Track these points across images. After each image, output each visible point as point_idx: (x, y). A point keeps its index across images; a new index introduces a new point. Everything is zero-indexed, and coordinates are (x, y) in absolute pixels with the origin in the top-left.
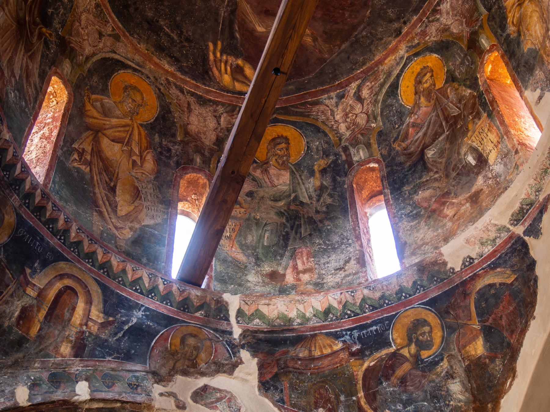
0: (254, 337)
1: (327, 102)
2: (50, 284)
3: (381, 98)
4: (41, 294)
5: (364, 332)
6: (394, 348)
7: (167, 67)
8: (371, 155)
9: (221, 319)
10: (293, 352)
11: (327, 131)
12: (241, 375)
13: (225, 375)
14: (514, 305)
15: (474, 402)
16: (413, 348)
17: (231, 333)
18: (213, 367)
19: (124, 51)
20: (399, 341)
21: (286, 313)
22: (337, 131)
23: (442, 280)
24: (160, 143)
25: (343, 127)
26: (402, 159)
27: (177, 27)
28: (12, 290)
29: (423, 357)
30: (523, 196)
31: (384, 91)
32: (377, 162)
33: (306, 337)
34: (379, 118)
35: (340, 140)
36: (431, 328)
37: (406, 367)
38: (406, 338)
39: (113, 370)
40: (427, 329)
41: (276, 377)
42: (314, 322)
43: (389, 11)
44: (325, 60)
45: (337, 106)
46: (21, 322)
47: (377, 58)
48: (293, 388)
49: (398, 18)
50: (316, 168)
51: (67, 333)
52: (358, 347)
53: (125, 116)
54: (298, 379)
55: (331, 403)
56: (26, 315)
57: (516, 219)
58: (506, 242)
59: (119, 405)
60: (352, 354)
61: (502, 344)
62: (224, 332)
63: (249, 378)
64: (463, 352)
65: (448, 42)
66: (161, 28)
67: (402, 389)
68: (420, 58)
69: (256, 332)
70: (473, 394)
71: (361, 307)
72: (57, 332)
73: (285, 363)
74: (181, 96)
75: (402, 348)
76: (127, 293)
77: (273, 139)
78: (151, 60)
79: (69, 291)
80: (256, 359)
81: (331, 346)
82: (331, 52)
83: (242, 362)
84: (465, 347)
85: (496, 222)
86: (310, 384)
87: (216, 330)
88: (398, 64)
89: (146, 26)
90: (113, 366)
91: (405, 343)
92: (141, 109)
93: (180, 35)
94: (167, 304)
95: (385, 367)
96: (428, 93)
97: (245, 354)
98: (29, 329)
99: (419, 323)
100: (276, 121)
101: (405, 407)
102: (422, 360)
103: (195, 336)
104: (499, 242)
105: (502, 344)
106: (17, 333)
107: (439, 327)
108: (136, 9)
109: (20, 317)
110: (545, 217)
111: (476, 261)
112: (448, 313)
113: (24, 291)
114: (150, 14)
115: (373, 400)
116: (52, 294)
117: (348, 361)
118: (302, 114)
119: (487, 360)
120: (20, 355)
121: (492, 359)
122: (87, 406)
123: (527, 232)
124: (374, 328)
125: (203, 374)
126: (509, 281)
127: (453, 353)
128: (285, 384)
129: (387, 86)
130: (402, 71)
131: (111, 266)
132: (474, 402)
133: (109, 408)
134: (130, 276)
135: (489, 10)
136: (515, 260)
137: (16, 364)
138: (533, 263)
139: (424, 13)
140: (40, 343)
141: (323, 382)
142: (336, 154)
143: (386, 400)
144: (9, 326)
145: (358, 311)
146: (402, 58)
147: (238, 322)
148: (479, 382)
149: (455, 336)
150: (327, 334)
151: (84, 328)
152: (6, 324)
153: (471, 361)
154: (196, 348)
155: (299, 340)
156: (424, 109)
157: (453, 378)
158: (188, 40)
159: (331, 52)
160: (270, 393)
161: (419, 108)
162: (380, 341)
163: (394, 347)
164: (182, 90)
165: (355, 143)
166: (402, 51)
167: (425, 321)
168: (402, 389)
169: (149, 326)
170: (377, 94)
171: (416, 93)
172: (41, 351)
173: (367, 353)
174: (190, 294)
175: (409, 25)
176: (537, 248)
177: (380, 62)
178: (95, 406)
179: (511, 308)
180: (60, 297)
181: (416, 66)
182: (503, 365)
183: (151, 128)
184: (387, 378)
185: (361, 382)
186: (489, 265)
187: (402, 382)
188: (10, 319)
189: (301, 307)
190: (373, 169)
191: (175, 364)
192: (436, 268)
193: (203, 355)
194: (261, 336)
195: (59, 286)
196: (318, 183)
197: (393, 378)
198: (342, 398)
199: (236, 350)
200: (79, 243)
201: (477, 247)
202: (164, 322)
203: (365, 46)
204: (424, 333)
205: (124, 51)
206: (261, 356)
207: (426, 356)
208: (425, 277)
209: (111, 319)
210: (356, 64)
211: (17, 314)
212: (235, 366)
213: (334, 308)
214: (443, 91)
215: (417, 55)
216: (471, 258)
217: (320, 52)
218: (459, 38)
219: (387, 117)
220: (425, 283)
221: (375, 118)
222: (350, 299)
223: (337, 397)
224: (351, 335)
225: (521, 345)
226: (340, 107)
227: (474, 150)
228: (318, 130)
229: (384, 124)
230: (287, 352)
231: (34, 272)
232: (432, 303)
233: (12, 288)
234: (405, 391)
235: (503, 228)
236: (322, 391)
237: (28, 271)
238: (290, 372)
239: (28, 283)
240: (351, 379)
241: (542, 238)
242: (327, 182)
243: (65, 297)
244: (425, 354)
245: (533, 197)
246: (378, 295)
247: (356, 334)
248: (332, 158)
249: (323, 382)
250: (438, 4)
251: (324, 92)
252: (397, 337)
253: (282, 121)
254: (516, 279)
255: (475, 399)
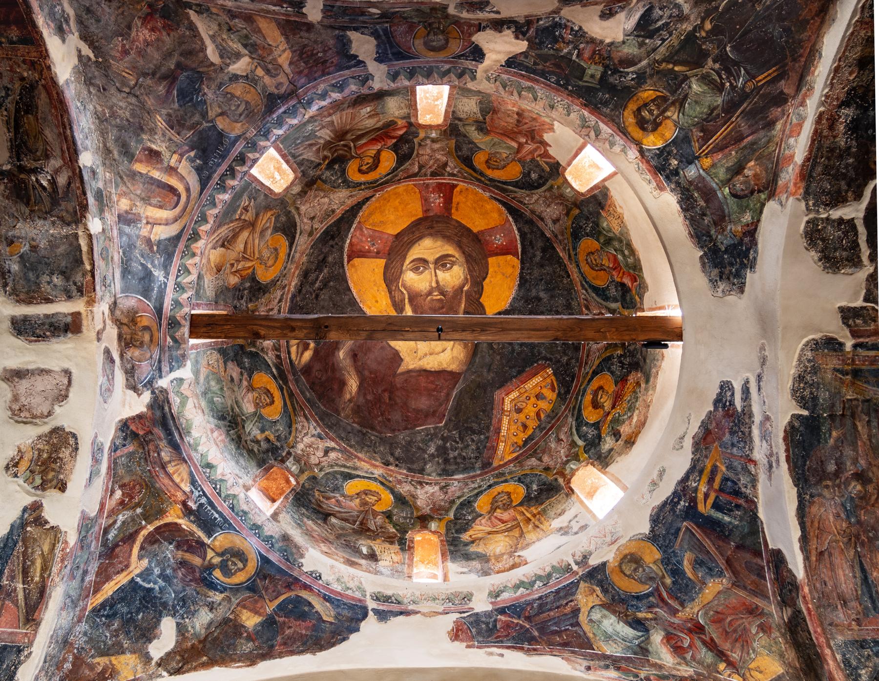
0: (164, 401)
1: (312, 427)
2: (182, 178)
3: (336, 469)
4: (172, 170)
5: (209, 508)
6: (208, 541)
7: (293, 284)
8: (298, 476)
9: (170, 363)
10: (163, 444)
11: (293, 434)
12: (128, 398)
13: (125, 381)
14: (308, 633)
15: (200, 642)
16: (217, 560)
17: (161, 377)
18: (129, 366)
19: (303, 242)
20: (217, 543)
21: (194, 427)
22: (296, 442)
23: (287, 560)
24: (245, 289)
25: (300, 446)
26: (313, 501)
27: (325, 285)
28: (175, 139)
29: (214, 573)
30: (400, 593)
31: (342, 469)
32: (298, 483)
33: (180, 453)
34: (323, 473)
35: (293, 447)
36: (243, 569)
37: (197, 561)
38: (223, 550)
39: (112, 258)
40: (240, 565)
41: (135, 435)
42: (196, 456)
43: (399, 450)
44: (339, 414)
45: (313, 436)
46: (147, 152)
47: (360, 455)
48: (130, 455)
49: (397, 459)
50: (267, 433)
51: (138, 204)
52: (194, 507)
53: (260, 252)
54: (140, 459)
55: (130, 500)
56: (153, 156)
57: (377, 598)
58: (353, 598)
59: (88, 267)
60: (184, 504)
61: (268, 640)
62: (160, 369)
63: (127, 407)
64: (239, 608)
65: (407, 502)
66: (321, 271)
67: (175, 566)
68: (382, 487)
69: (168, 402)
70: (207, 637)
71: (228, 496)
72: (139, 192)
73: (151, 440)
74: (276, 301)
75: (212, 549)
76: (176, 261)
77: (268, 391)
78: (296, 268)
79: (176, 198)
80: (145, 410)
81: (182, 480)
82: (347, 417)
83: (139, 395)
84: (244, 607)
85: (363, 583)
86: (140, 472)
87: (160, 361)
88: (366, 472)
89: (321, 258)
90: (116, 258)
91: (219, 550)
92: (263, 267)
93: (320, 289)
94: (172, 305)
95: (188, 541)
96: (364, 503)
97: (147, 397)
98: (141, 161)
99: (240, 555)
100: (282, 389)
101: (159, 576)
102: (210, 574)
103: (151, 340)
104: (349, 592)
105: (268, 640)
106: (137, 148)
107: (249, 576)
108: (332, 246)
109: (151, 151)
110: (401, 618)
111: (320, 582)
112: (265, 578)
113: (175, 152)
114: (330, 259)
115: (150, 541)
116: (174, 182)
117: (176, 502)
118: (294, 409)
119: (245, 635)
120: (116, 153)
121: (249, 638)
122: (80, 233)
123: (376, 612)
124: (217, 516)
125: (122, 356)
126: (325, 618)
127: (233, 599)
128: (131, 448)
129: (346, 470)
130: (364, 477)
131: (196, 241)
132: (200, 642)
133: (81, 258)
134: (190, 261)
135: (456, 518)
136: (346, 613)
137: (107, 151)
138: (358, 630)
139: (413, 477)
140: (128, 176)
141: (147, 485)
142: (282, 446)
143: (156, 555)
144: (143, 139)
145: (223, 495)
146: (373, 474)
147: (172, 382)
148: (221, 637)
149: (248, 594)
150: (191, 474)
151: (145, 221)
152: (145, 137)
153: (235, 620)
154: (142, 344)
155: (176, 447)
156: (352, 504)
157: (211, 610)
158: (317, 296)
159: (347, 417)
160: (120, 433)
161: (351, 500)
162: (209, 526)
163: (209, 542)
164: (280, 301)
165: (298, 460)
166: (378, 472)
167: (247, 560)
168: (175, 566)
169: (153, 290)
170: (337, 465)
171: (357, 494)
172: (121, 178)
173: (192, 518)
174: (184, 326)
175: (397, 469)
176: (370, 625)
177: (359, 459)
178: (83, 243)
179: (304, 632)
180: (170, 191)
181: (374, 486)
182: (251, 652)
183: (253, 279)
184: (178, 547)
185: (162, 523)
186: (325, 595)
187: (181, 563)
188: (149, 140)
189: (204, 440)
190: (288, 481)
191: (125, 324)
192: (294, 550)
193: (137, 353)
194: (166, 408)
195: (180, 188)
196: (259, 438)
197: (180, 552)
198: (139, 511)
199: (149, 386)
200: (214, 204)
201: (333, 577)
202: (158, 305)
203: (364, 443)
204: (236, 565)
205: (303, 242)
206: (150, 413)
207: (216, 575)
208: (280, 544)
209: (155, 248)
210: (347, 440)
211: (154, 147)
212: (134, 389)
213: (216, 471)
214: (375, 514)
215: (382, 483)
216: (320, 576)
217: (343, 409)
218: (418, 509)
219: (328, 479)
220: (277, 546)
221: (321, 470)
222: (229, 483)
223: (138, 505)
224: (200, 496)
225: (281, 657)
226: (313, 439)
227: (370, 548)
228: (290, 427)
229: (322, 478)
230: (161, 440)
231: (192, 160)
232: (265, 560)
233: (177, 138)
234: (174, 570)
235: (364, 592)
236: (138, 487)
237: (192, 154)
238: (144, 448)
239: (182, 155)
240: (161, 512)
241: (382, 625)
242: (264, 445)
243: (171, 195)
244: (217, 573)
245: (406, 601)
246: (245, 507)
247: (203, 500)
248: (278, 444)
249: (147, 485)
250: (427, 484)
251: (316, 421)
252: (220, 540)
253: (283, 394)
254: (331, 623)
255: (203, 641)
